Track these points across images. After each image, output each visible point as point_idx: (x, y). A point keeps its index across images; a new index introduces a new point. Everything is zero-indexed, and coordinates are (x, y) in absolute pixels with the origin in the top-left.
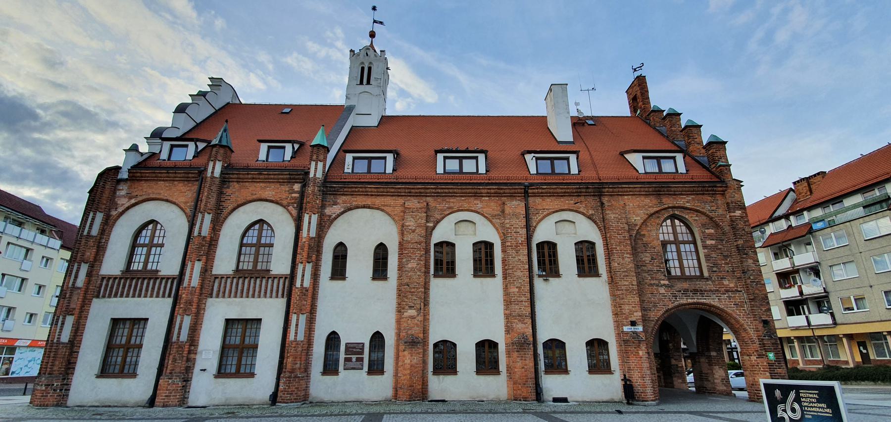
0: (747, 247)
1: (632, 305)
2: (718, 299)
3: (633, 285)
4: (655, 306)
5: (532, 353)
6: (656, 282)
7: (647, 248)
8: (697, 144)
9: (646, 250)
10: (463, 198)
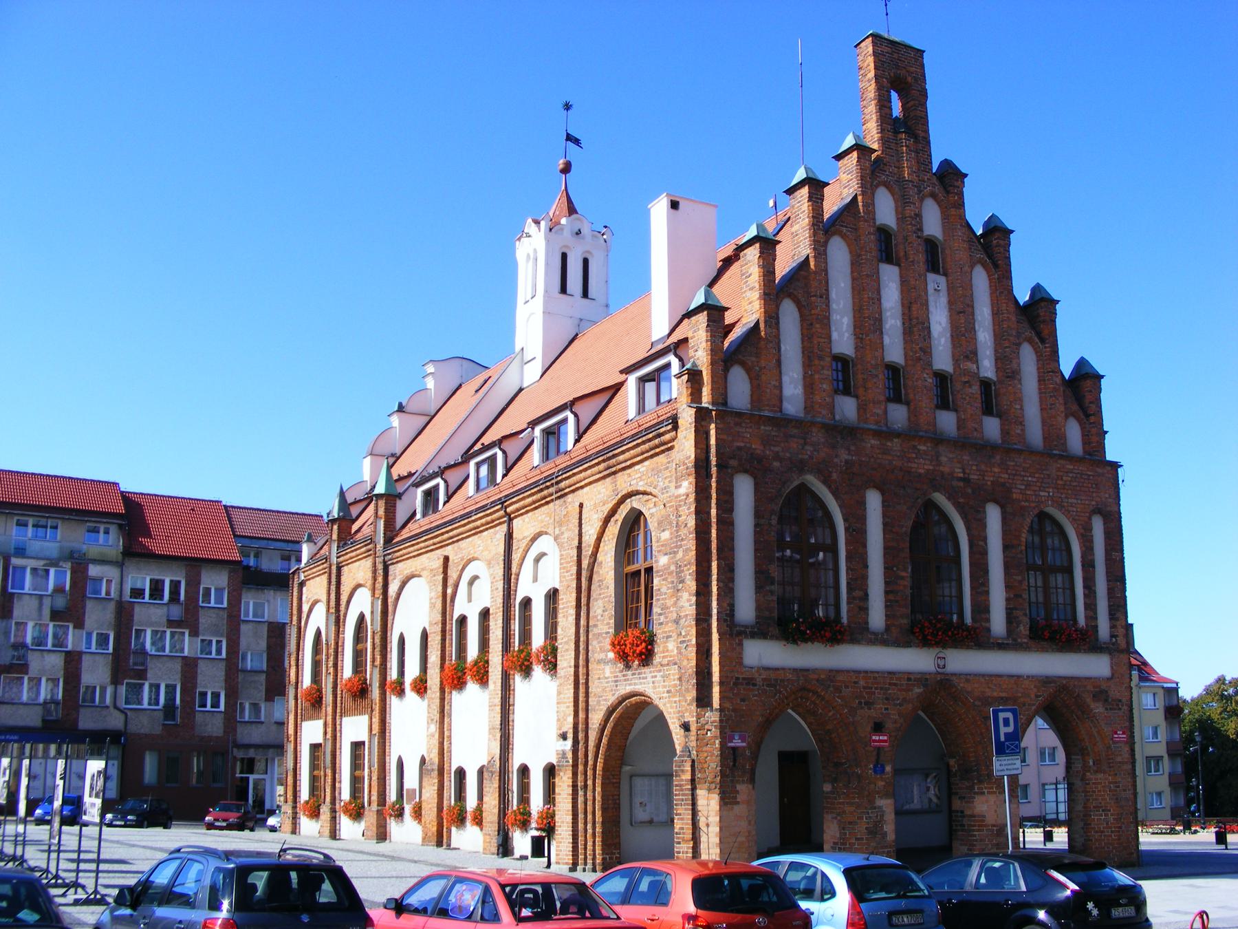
0: (686, 565)
1: (566, 703)
2: (653, 682)
3: (570, 667)
4: (599, 702)
5: (497, 786)
6: (602, 656)
7: (601, 589)
8: (750, 289)
9: (600, 594)
10: (470, 539)
